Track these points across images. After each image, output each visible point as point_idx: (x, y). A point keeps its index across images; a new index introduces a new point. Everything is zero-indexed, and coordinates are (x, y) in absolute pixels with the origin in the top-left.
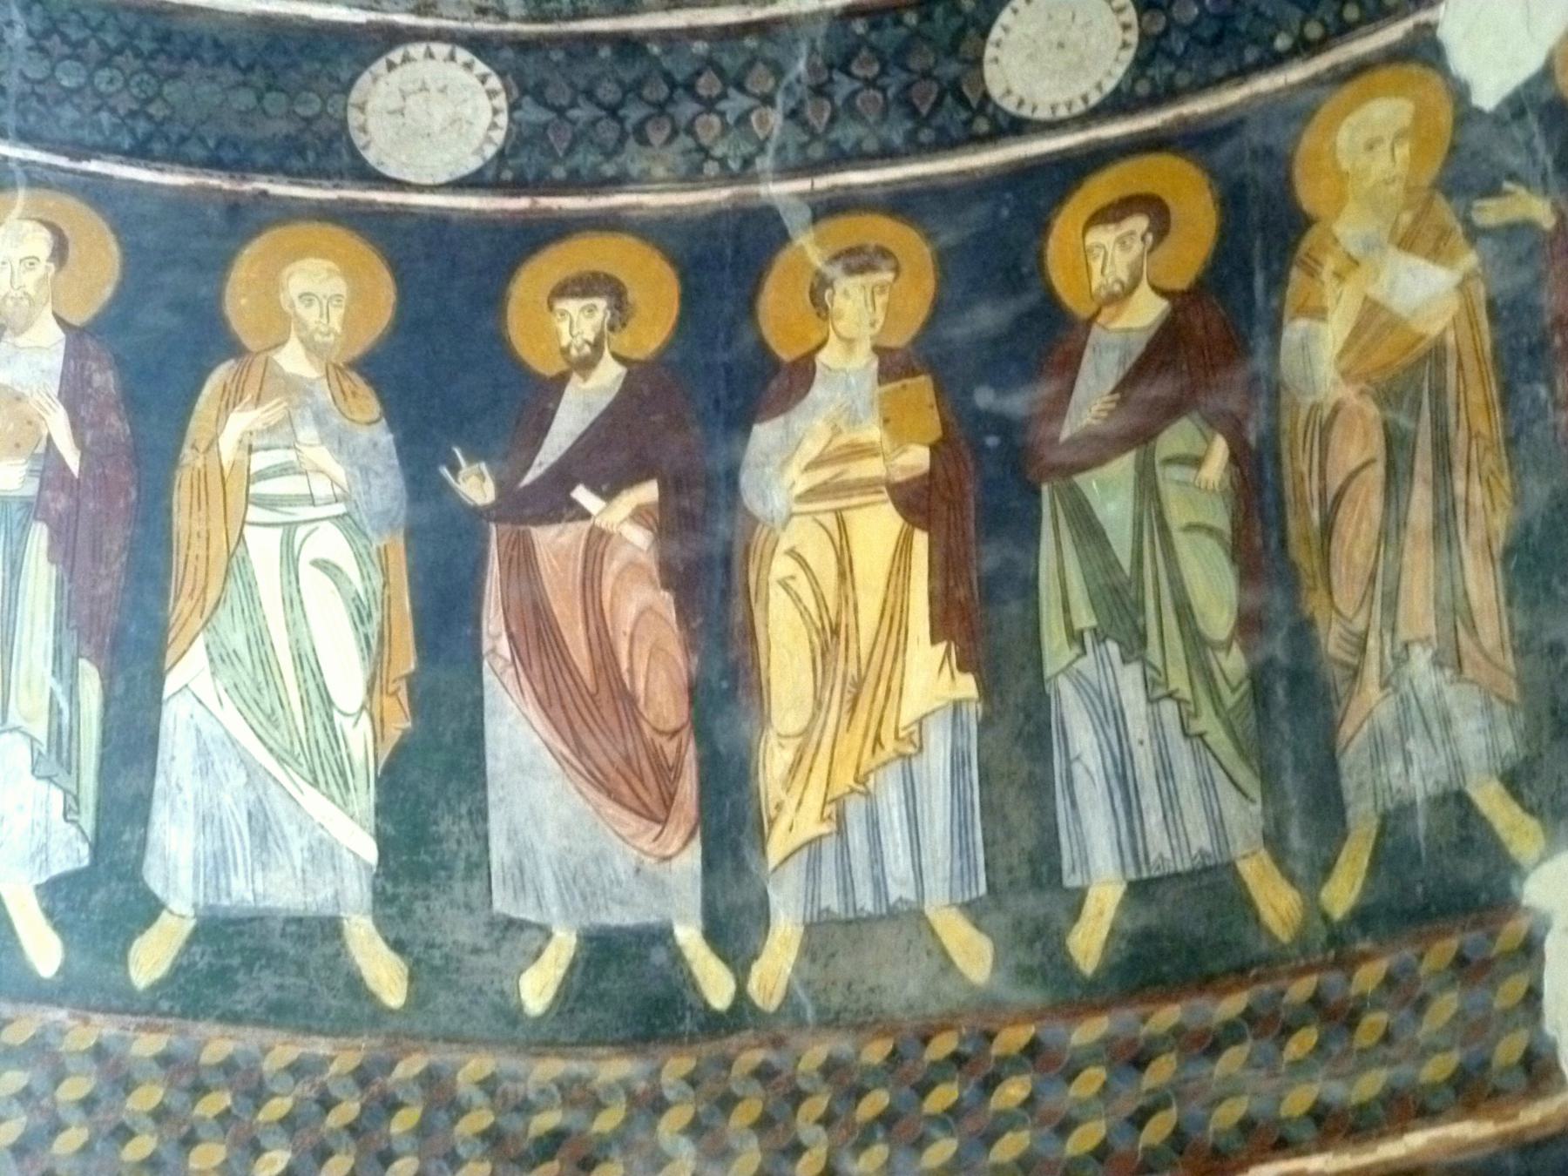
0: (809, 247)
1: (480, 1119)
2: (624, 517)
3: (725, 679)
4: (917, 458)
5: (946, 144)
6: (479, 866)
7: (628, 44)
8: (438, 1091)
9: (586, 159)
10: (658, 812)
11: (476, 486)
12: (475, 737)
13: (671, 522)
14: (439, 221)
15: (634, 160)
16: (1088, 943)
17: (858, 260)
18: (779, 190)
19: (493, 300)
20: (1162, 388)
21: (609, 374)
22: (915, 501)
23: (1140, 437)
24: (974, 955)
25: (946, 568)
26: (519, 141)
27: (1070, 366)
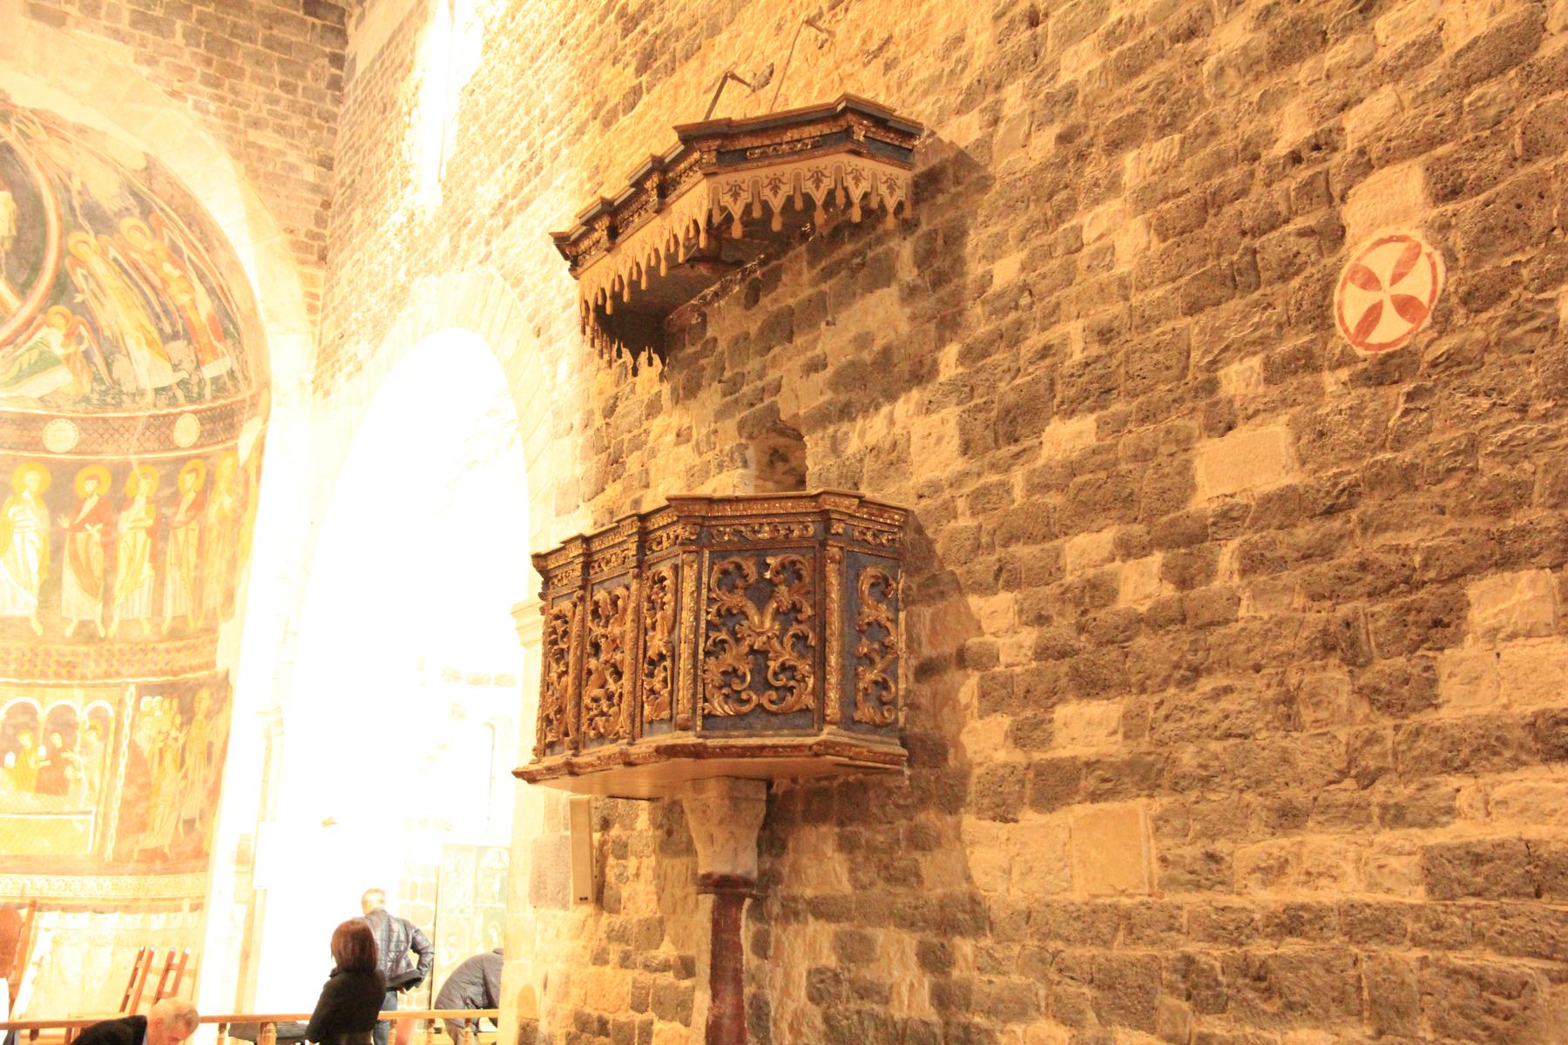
0: (137, 471)
1: (55, 658)
2: (94, 530)
3: (111, 568)
4: (151, 522)
5: (165, 450)
6: (59, 606)
7: (105, 420)
8: (47, 652)
9: (95, 447)
10: (95, 595)
11: (65, 523)
12: (60, 579)
13: (105, 533)
14: (61, 462)
15: (105, 448)
16: (165, 629)
17: (145, 475)
18: (133, 458)
19: (72, 479)
20: (192, 513)
21: (95, 499)
22: (151, 532)
23: (186, 523)
24: (147, 629)
25: (154, 546)
26: (82, 442)
27: (178, 505)
